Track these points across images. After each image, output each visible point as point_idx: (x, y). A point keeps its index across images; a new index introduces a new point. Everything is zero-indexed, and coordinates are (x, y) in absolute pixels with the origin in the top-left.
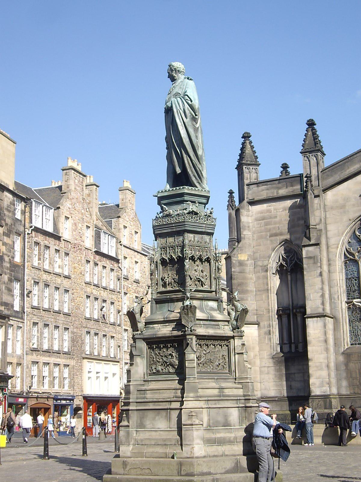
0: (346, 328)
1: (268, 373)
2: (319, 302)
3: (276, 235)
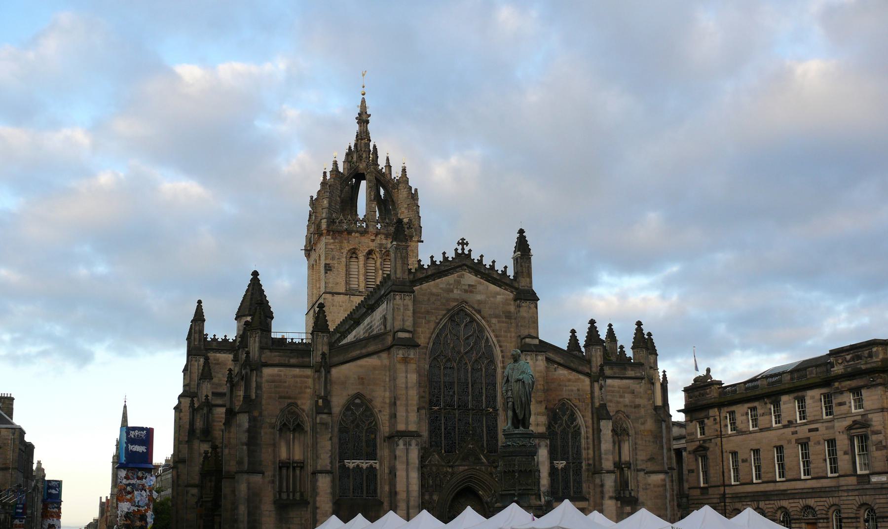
2: (328, 461)
3: (285, 398)
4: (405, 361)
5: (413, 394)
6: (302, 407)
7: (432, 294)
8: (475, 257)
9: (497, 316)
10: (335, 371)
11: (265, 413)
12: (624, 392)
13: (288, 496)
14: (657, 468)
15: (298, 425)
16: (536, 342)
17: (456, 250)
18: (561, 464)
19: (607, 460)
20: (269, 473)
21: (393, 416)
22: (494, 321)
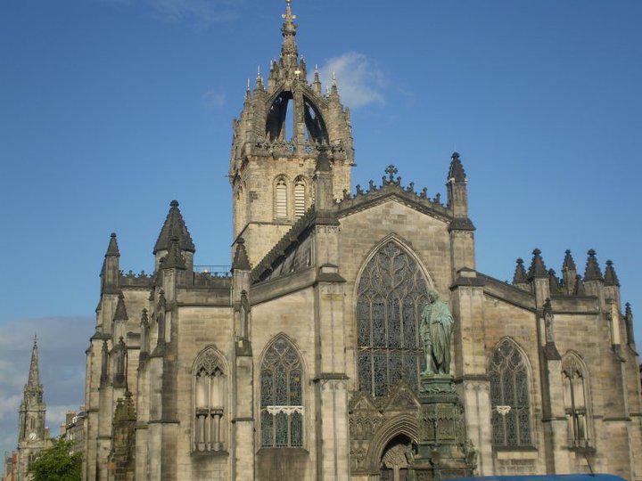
0: (259, 430)
1: (185, 470)
3: (202, 340)
4: (330, 297)
5: (339, 332)
6: (221, 350)
7: (359, 226)
8: (405, 184)
9: (429, 248)
10: (255, 311)
11: (181, 357)
12: (575, 329)
13: (206, 446)
14: (617, 415)
15: (217, 369)
16: (473, 275)
17: (384, 178)
18: (504, 410)
19: (557, 405)
20: (185, 423)
21: (319, 357)
22: (426, 253)
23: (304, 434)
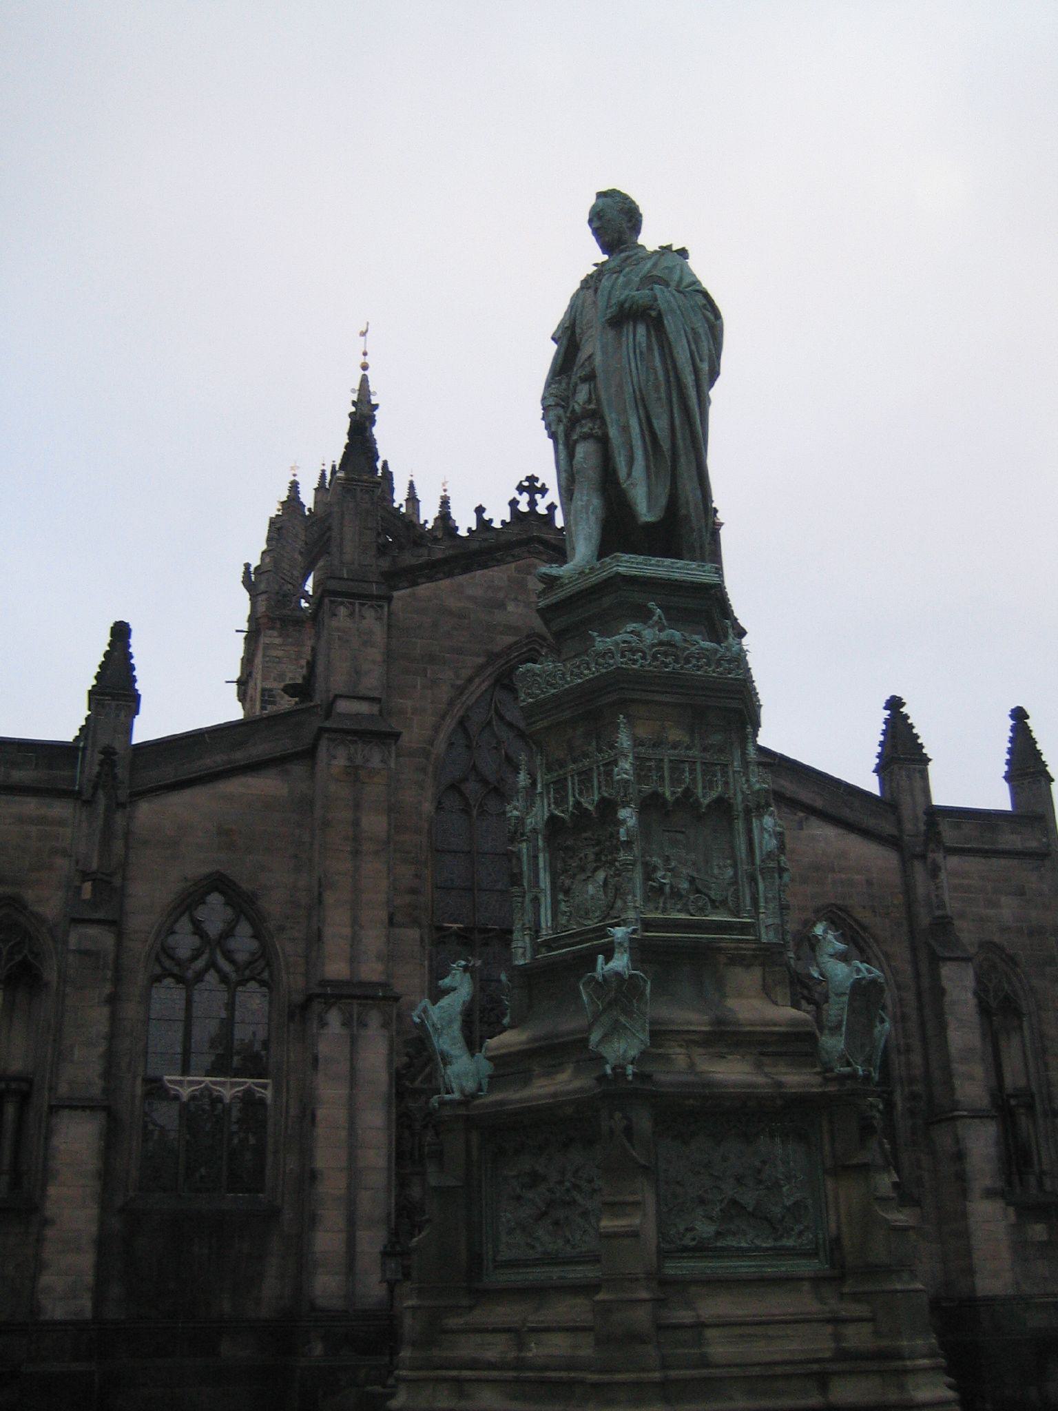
10: (145, 811)
17: (514, 503)
21: (317, 937)
23: (270, 1159)
